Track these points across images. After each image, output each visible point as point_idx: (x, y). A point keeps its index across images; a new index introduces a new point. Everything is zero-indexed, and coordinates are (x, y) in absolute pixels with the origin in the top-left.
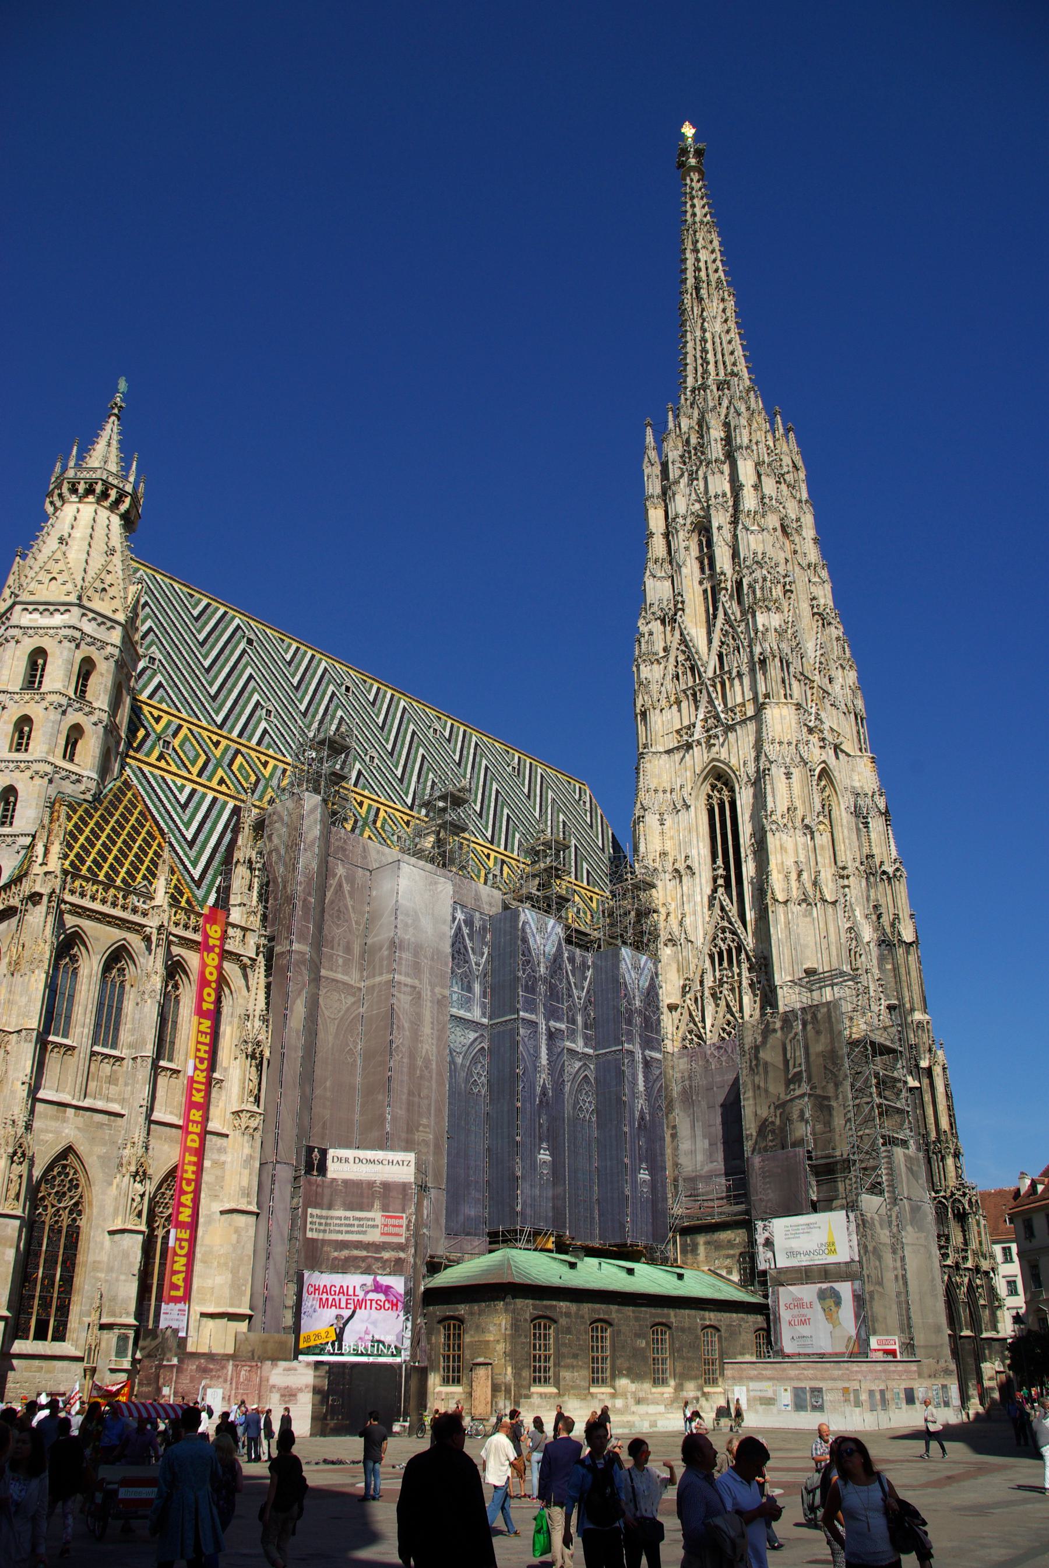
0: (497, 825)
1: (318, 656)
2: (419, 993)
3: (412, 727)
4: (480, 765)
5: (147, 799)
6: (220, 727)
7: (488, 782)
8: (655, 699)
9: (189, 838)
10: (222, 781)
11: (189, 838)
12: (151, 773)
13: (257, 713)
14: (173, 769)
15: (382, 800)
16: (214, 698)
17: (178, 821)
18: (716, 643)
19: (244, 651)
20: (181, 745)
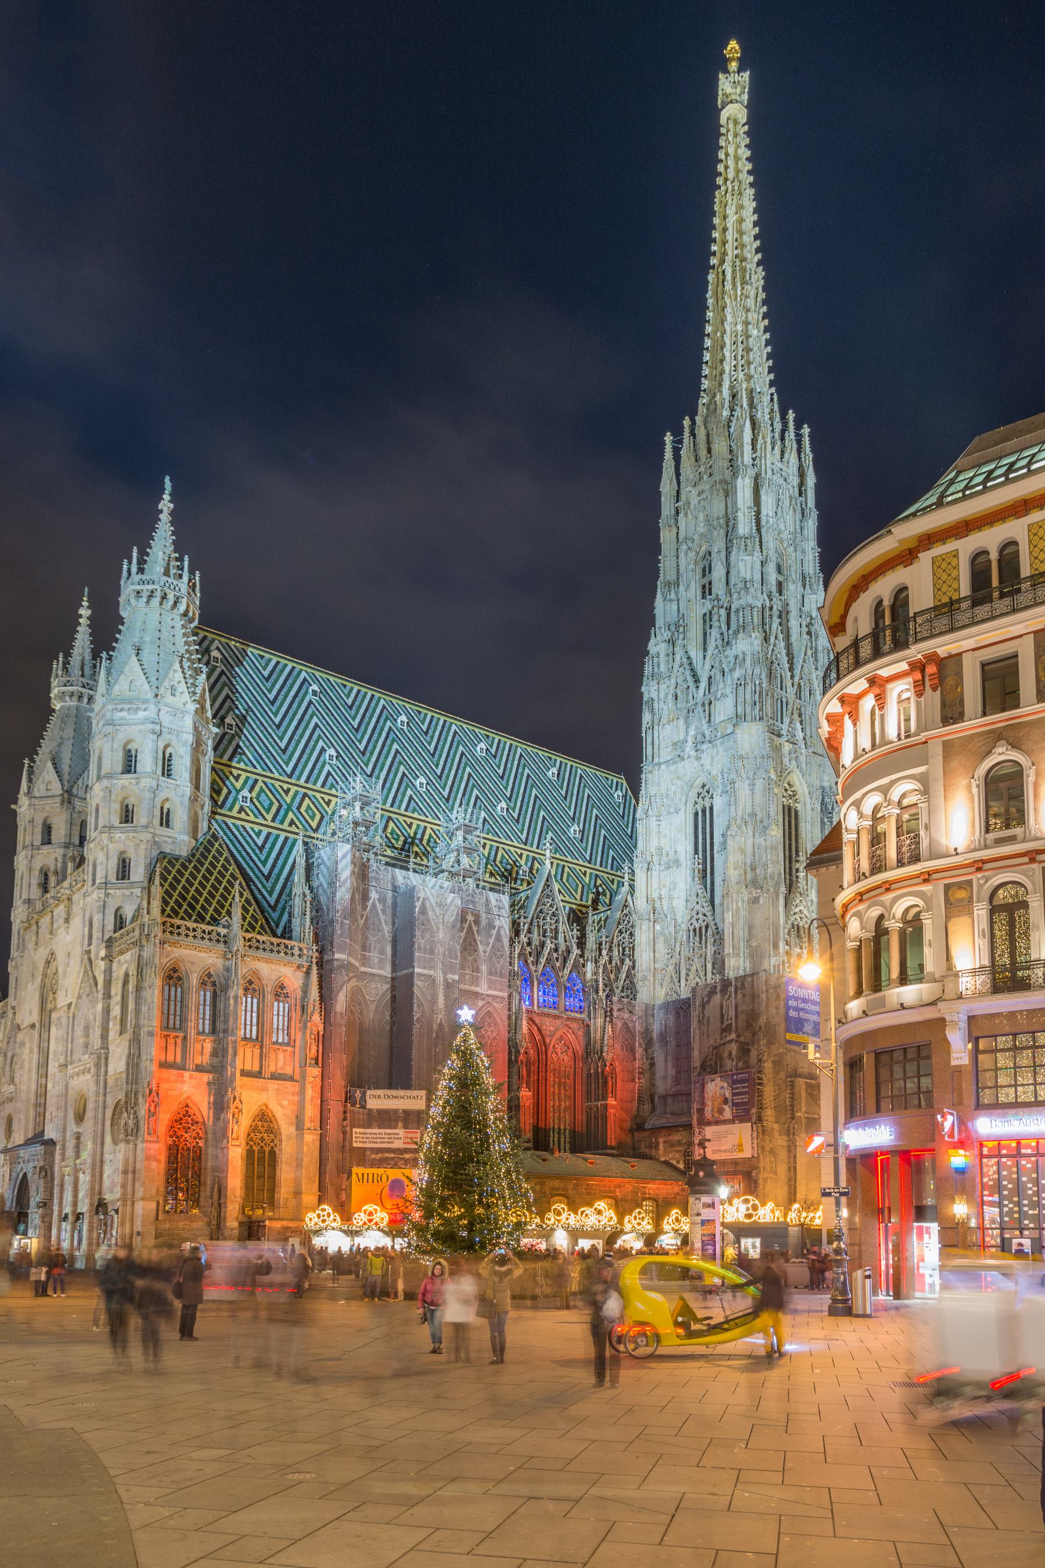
0: (533, 826)
1: (377, 695)
2: (434, 980)
3: (461, 748)
4: (522, 774)
5: (231, 846)
6: (290, 776)
7: (528, 790)
8: (656, 718)
9: (266, 872)
10: (292, 823)
11: (266, 872)
12: (234, 824)
13: (322, 759)
14: (252, 818)
15: (430, 819)
16: (284, 751)
17: (257, 861)
18: (708, 666)
19: (311, 702)
20: (257, 798)
